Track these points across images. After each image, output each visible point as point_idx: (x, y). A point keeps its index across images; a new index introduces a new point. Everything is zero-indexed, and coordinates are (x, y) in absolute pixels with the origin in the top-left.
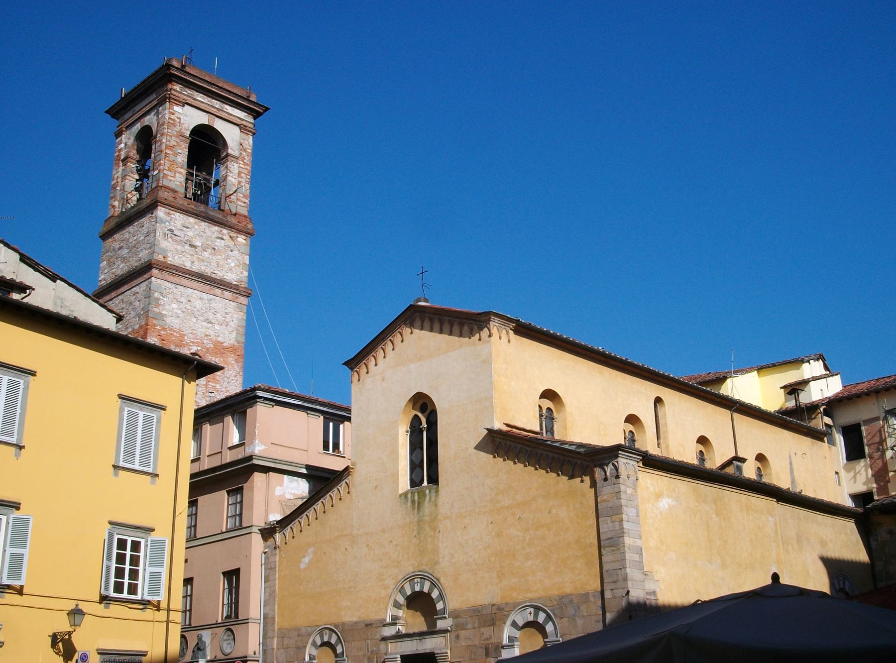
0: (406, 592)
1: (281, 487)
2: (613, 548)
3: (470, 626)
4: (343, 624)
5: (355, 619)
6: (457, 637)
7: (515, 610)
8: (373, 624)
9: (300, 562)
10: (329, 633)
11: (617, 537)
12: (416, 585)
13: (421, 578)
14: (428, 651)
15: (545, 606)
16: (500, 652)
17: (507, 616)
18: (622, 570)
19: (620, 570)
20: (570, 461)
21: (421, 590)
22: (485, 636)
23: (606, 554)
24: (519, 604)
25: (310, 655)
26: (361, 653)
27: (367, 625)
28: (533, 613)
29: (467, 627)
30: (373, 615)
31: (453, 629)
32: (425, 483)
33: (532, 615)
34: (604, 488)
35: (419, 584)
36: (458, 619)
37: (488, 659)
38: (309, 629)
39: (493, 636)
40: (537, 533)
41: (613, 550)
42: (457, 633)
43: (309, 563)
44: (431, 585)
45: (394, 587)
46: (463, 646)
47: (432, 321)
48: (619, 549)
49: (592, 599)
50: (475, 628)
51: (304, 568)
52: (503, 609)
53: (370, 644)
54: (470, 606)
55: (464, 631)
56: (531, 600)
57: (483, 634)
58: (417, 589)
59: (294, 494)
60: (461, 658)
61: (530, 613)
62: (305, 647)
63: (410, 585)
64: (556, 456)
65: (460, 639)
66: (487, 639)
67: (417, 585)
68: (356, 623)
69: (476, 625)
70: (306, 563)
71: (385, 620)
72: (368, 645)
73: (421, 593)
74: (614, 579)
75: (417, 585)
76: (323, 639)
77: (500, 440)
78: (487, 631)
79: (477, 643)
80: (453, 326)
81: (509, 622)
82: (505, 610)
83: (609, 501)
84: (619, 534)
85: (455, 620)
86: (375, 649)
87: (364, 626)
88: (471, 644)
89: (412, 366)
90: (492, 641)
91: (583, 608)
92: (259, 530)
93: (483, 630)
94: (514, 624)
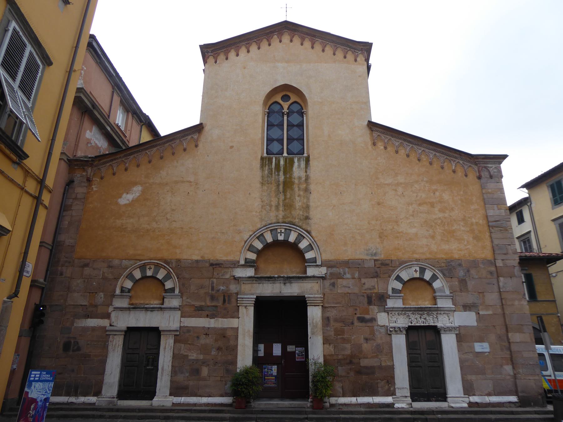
0: (266, 240)
1: (90, 131)
2: (501, 229)
3: (348, 276)
4: (179, 261)
5: (195, 258)
6: (333, 285)
7: (402, 267)
8: (222, 264)
9: (121, 197)
10: (154, 267)
11: (504, 221)
12: (279, 235)
13: (286, 229)
14: (296, 295)
15: (433, 267)
16: (386, 302)
17: (393, 271)
18: (512, 246)
19: (509, 246)
20: (452, 160)
21: (286, 239)
22: (366, 286)
23: (495, 232)
24: (406, 262)
25: (122, 287)
26: (202, 292)
27: (212, 265)
28: (419, 271)
29: (345, 277)
30: (220, 256)
31: (328, 277)
32: (285, 154)
33: (418, 273)
34: (488, 184)
35: (283, 234)
36: (334, 269)
37: (371, 307)
38: (125, 262)
39: (376, 287)
40: (421, 208)
41: (501, 230)
42: (332, 281)
43: (132, 201)
44: (298, 236)
45: (251, 233)
46: (339, 293)
47: (303, 40)
48: (507, 230)
49: (481, 266)
50: (355, 278)
51: (125, 205)
52: (388, 265)
53: (215, 283)
54: (348, 258)
55: (339, 280)
56: (417, 260)
57: (364, 284)
58: (281, 238)
59: (96, 144)
60: (337, 303)
61: (416, 271)
62: (117, 279)
63: (272, 234)
64: (437, 154)
65: (336, 287)
66: (370, 289)
67: (281, 235)
68: (197, 261)
69: (357, 275)
70: (128, 200)
71: (239, 262)
72: (213, 283)
73: (285, 244)
74: (505, 252)
75: (281, 235)
76: (157, 273)
77: (379, 134)
78: (370, 283)
79: (356, 290)
80: (325, 46)
81: (394, 276)
82: (391, 265)
83: (493, 194)
84: (505, 219)
85: (330, 269)
86: (222, 288)
87: (207, 265)
88: (350, 292)
89: (279, 65)
90: (376, 291)
91: (473, 272)
92: (67, 159)
93: (363, 281)
94: (398, 278)
